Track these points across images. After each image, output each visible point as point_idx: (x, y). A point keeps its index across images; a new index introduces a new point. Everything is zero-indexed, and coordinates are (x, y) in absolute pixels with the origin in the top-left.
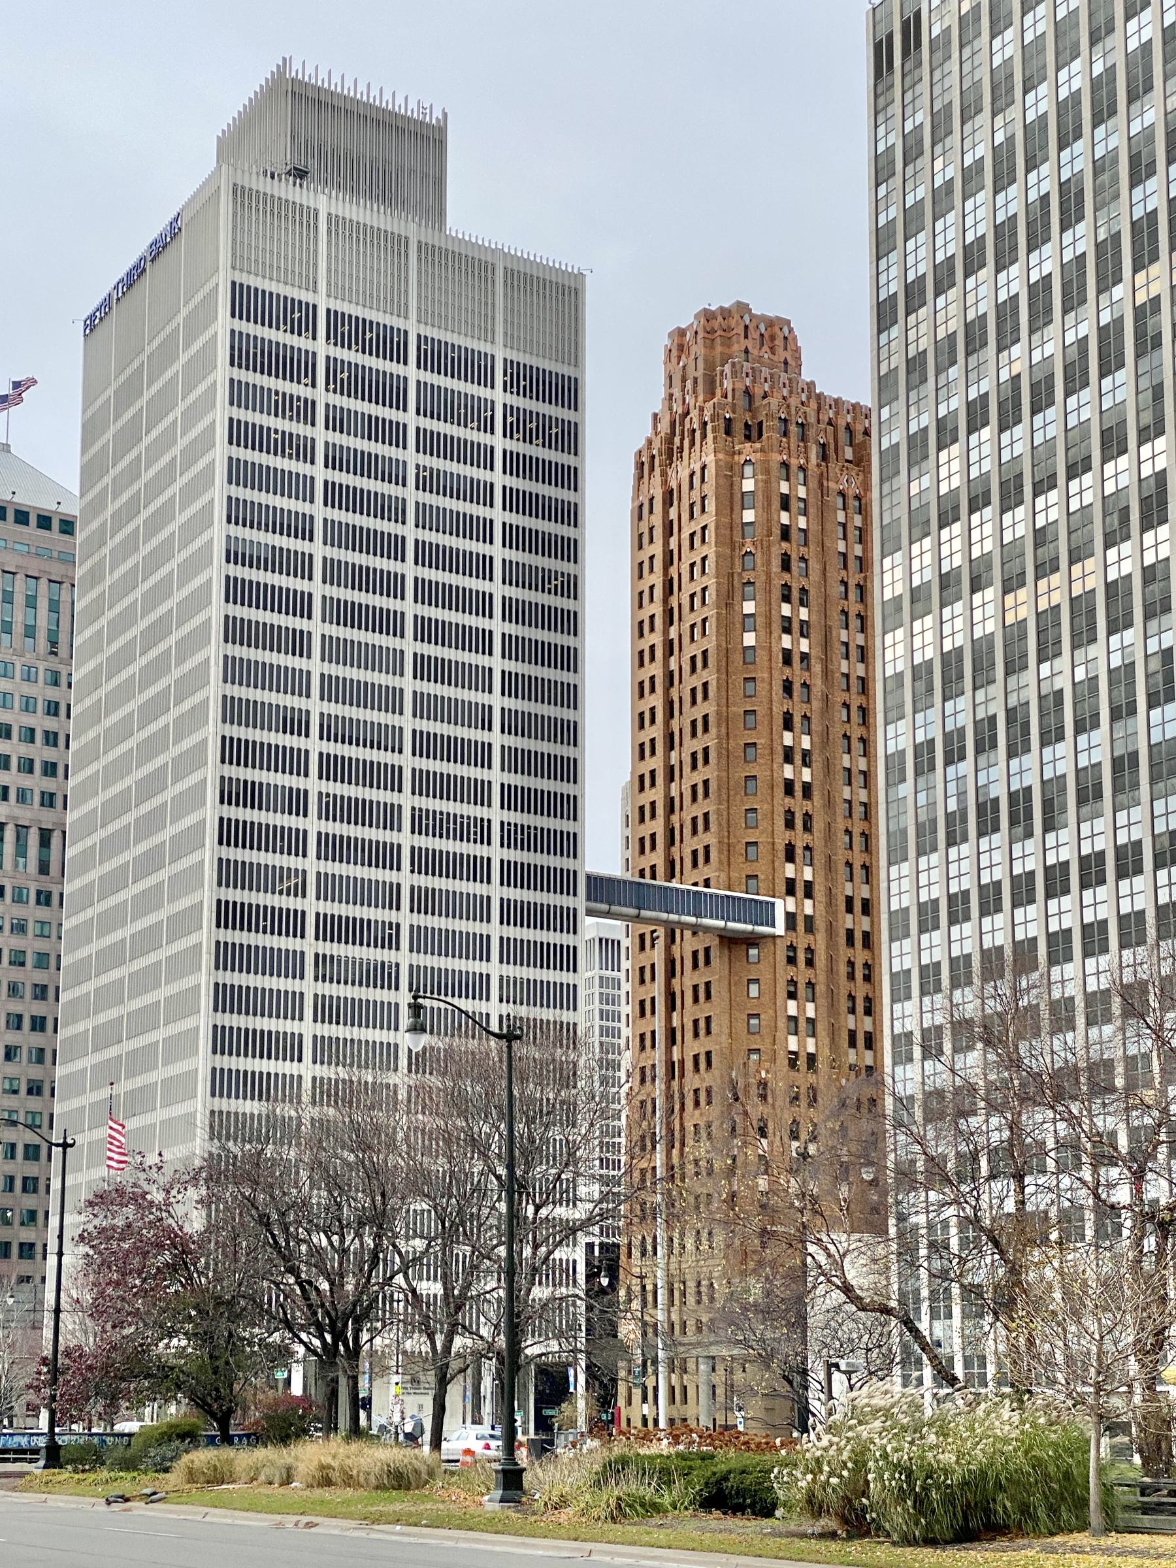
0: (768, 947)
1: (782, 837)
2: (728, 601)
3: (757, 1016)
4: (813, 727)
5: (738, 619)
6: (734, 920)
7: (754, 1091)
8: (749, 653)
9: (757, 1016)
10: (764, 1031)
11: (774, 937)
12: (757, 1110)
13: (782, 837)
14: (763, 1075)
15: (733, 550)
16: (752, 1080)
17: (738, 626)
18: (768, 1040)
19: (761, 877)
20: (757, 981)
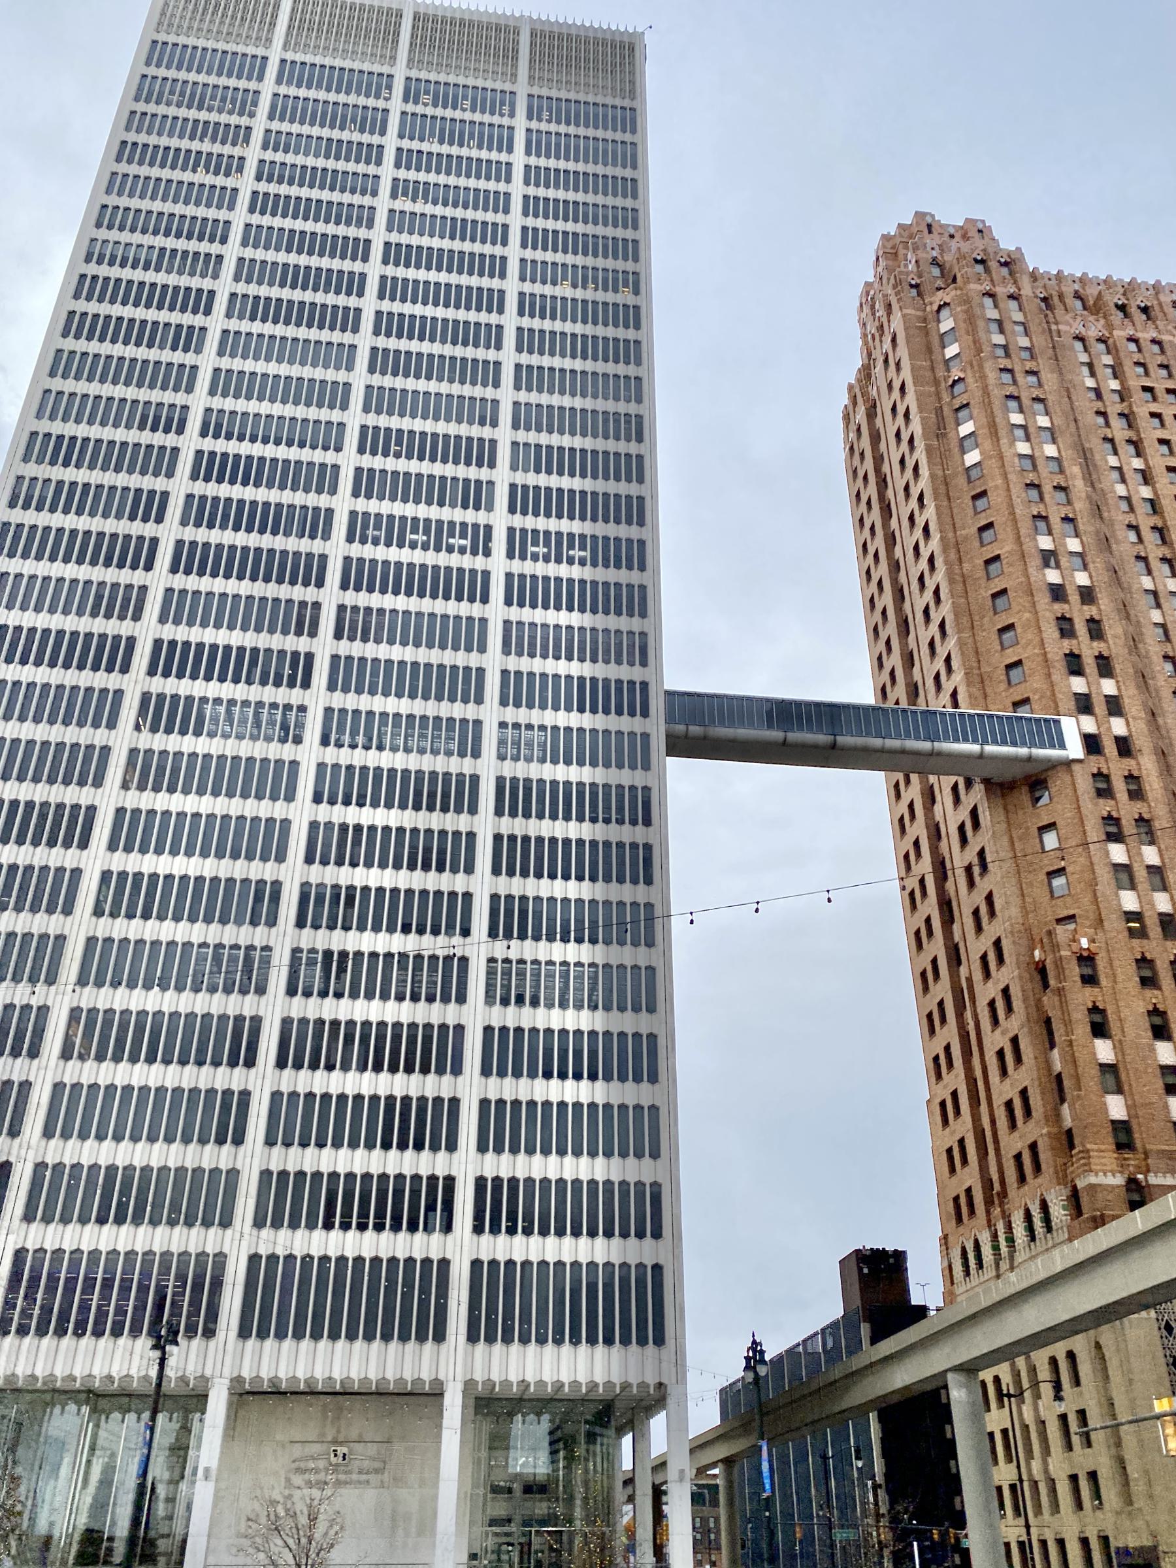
0: (1058, 782)
1: (1058, 648)
2: (939, 429)
3: (1061, 871)
4: (1081, 527)
5: (954, 444)
6: (995, 742)
7: (1074, 971)
8: (974, 474)
9: (1061, 871)
10: (1078, 888)
11: (1068, 764)
12: (1081, 997)
13: (1058, 648)
14: (1084, 943)
15: (936, 383)
16: (1065, 953)
17: (956, 450)
18: (1086, 900)
19: (1034, 698)
20: (1051, 826)
